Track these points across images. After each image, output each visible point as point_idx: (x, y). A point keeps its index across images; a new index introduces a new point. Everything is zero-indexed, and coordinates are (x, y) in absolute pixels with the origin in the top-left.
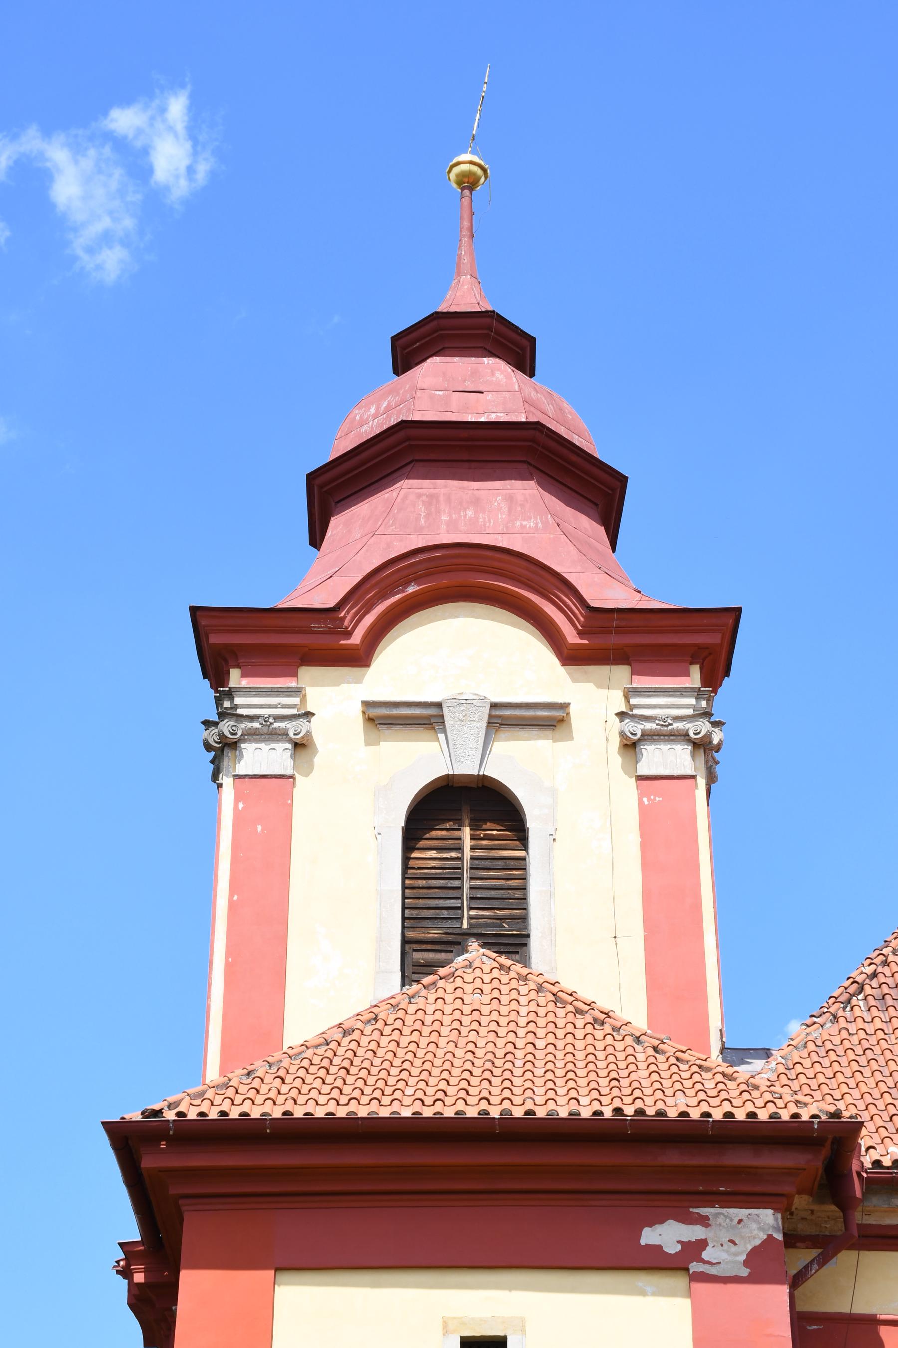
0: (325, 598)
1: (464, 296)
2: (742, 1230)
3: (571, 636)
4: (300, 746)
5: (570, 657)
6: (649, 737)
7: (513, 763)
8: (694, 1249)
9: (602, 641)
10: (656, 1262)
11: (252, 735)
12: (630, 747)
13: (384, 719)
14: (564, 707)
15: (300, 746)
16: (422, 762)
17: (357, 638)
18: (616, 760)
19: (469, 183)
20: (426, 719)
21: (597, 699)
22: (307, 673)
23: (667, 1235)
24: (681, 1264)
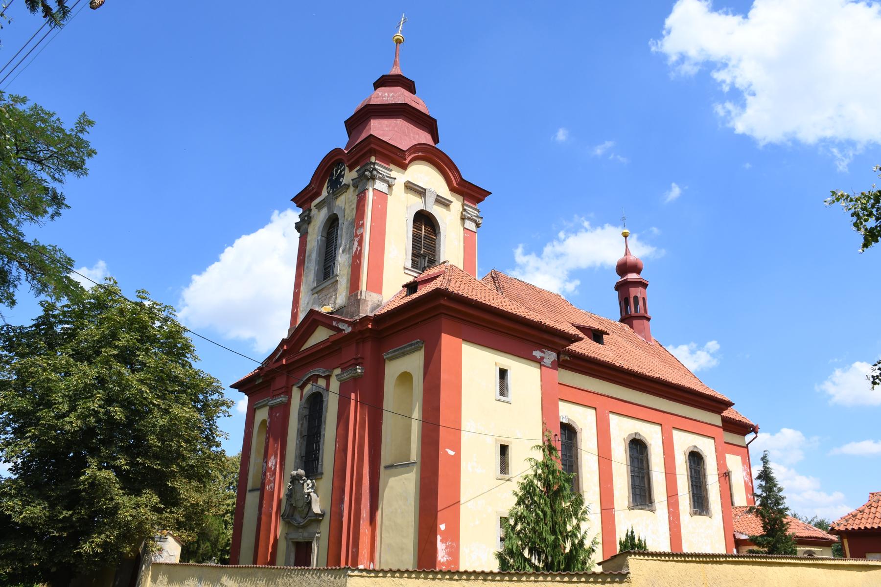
0: (404, 147)
1: (395, 71)
2: (550, 357)
3: (455, 184)
4: (390, 186)
5: (452, 189)
6: (469, 219)
7: (437, 211)
8: (542, 358)
9: (462, 189)
10: (534, 360)
11: (380, 179)
12: (463, 219)
13: (410, 187)
14: (451, 202)
15: (390, 186)
16: (416, 204)
17: (407, 162)
18: (459, 221)
19: (398, 42)
20: (421, 192)
21: (457, 204)
22: (392, 166)
23: (537, 354)
24: (539, 362)
